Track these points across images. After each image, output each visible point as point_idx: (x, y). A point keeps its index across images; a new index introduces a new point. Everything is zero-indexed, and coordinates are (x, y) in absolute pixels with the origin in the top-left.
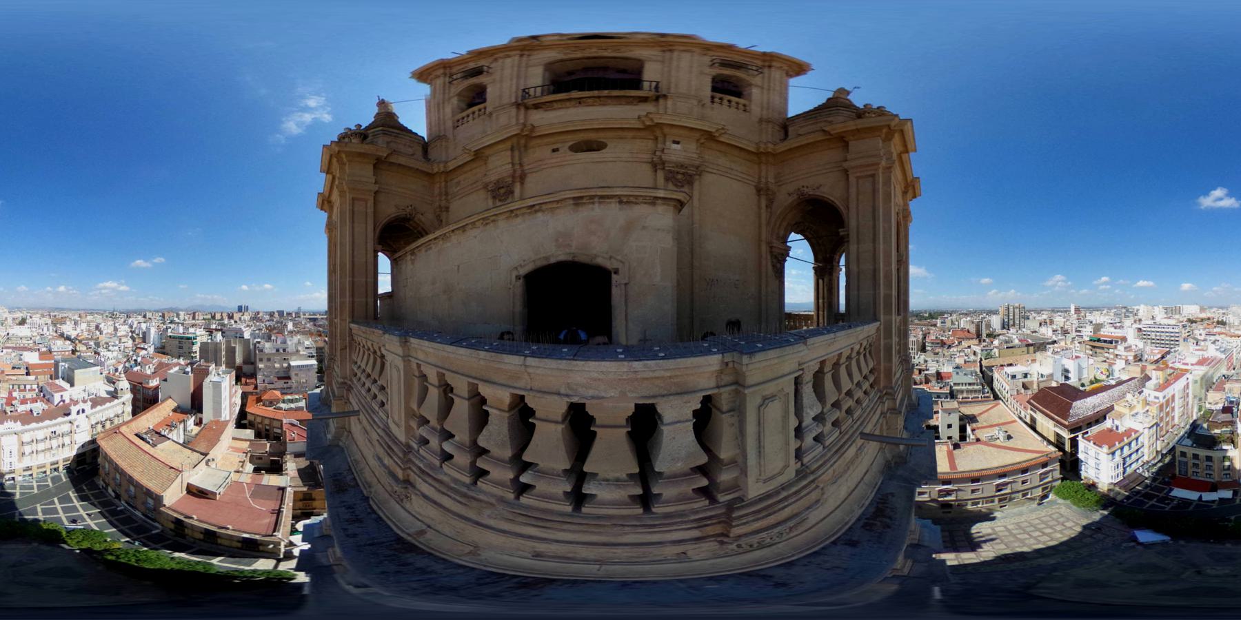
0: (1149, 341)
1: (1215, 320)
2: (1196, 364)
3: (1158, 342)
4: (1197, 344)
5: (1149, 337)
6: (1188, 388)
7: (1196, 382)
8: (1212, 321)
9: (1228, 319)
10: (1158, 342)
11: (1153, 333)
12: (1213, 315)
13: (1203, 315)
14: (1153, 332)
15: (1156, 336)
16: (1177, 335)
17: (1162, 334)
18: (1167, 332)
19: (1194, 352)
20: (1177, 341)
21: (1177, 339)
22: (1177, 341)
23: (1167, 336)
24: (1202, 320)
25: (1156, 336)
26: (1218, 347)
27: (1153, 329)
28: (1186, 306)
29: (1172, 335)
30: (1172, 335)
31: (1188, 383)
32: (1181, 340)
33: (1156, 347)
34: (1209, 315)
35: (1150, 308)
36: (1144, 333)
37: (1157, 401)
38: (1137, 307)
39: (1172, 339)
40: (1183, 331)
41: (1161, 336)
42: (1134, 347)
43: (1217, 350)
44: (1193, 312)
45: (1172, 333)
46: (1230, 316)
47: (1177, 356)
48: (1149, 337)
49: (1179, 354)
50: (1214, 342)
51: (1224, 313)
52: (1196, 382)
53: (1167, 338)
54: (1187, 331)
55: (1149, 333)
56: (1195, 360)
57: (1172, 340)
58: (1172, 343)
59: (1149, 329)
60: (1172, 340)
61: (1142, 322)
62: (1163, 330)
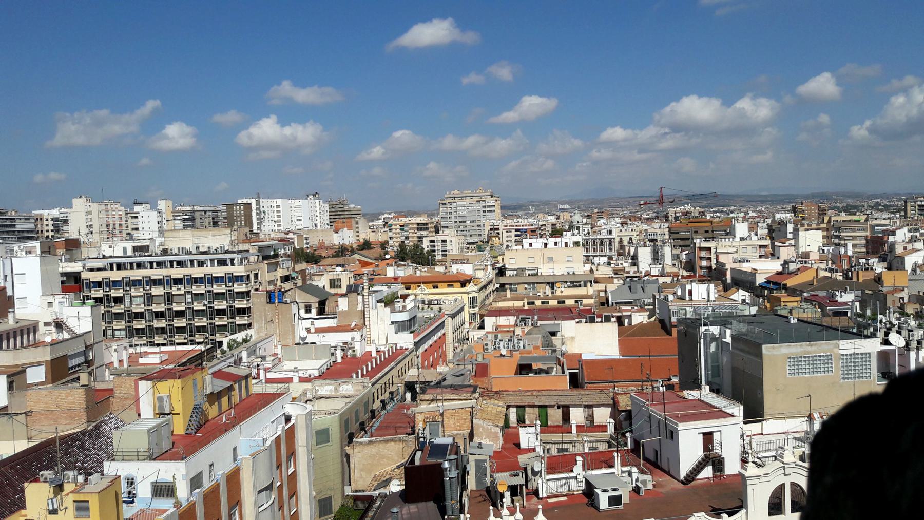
0: (122, 325)
1: (394, 244)
2: (321, 377)
3: (162, 323)
4: (321, 311)
5: (119, 309)
6: (292, 454)
7: (322, 436)
8: (378, 251)
9: (438, 248)
10: (162, 323)
11: (134, 292)
12: (381, 237)
13: (346, 237)
14: (137, 283)
15: (149, 299)
16: (237, 288)
17: (174, 290)
18: (197, 281)
19: (311, 338)
20: (242, 312)
21: (239, 304)
22: (242, 312)
23: (197, 297)
24: (342, 251)
25: (149, 299)
26: (403, 317)
27: (136, 274)
28: (274, 202)
29: (217, 289)
30: (217, 289)
31: (290, 434)
32: (258, 302)
33: (152, 344)
34: (366, 234)
35: (118, 210)
36: (100, 294)
37: (166, 504)
38: (55, 213)
39: (222, 305)
40: (265, 275)
41: (169, 298)
42: (48, 335)
43: (401, 327)
44: (306, 224)
45: (219, 280)
46: (444, 234)
47: (244, 355)
48: (119, 309)
49: (252, 352)
50: (389, 302)
51: (422, 227)
52: (322, 436)
53: (197, 306)
54: (280, 272)
55: (118, 293)
56: (314, 366)
57: (221, 312)
58: (218, 321)
59: (116, 275)
60: (221, 312)
61: (84, 253)
62: (177, 273)
